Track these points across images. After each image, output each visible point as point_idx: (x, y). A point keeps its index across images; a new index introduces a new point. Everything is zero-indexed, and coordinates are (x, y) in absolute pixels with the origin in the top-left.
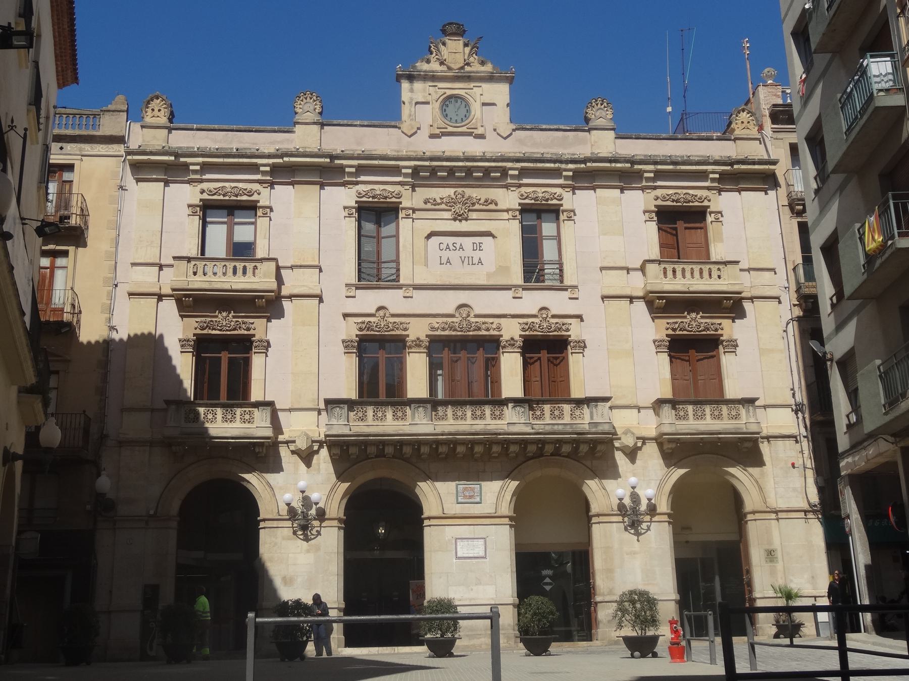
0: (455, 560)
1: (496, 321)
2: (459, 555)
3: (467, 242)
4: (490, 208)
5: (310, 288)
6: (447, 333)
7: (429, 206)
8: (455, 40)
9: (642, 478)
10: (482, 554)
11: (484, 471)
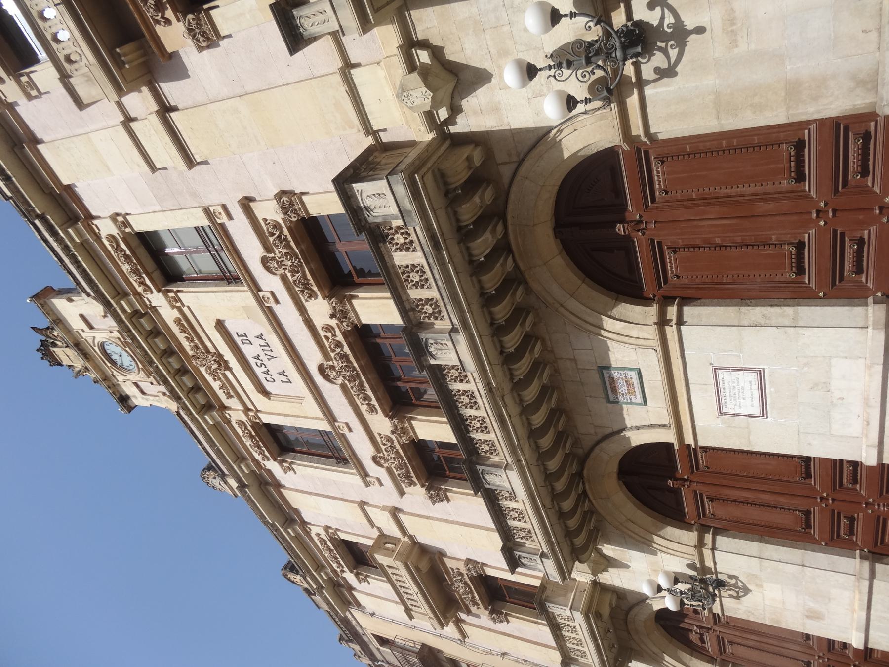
0: (769, 419)
1: (322, 333)
2: (757, 411)
3: (247, 350)
4: (187, 324)
5: (388, 520)
6: (370, 393)
7: (232, 393)
8: (58, 356)
9: (506, 29)
10: (753, 377)
11: (574, 360)
